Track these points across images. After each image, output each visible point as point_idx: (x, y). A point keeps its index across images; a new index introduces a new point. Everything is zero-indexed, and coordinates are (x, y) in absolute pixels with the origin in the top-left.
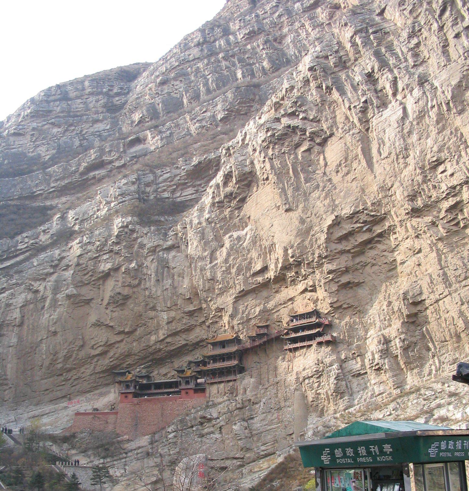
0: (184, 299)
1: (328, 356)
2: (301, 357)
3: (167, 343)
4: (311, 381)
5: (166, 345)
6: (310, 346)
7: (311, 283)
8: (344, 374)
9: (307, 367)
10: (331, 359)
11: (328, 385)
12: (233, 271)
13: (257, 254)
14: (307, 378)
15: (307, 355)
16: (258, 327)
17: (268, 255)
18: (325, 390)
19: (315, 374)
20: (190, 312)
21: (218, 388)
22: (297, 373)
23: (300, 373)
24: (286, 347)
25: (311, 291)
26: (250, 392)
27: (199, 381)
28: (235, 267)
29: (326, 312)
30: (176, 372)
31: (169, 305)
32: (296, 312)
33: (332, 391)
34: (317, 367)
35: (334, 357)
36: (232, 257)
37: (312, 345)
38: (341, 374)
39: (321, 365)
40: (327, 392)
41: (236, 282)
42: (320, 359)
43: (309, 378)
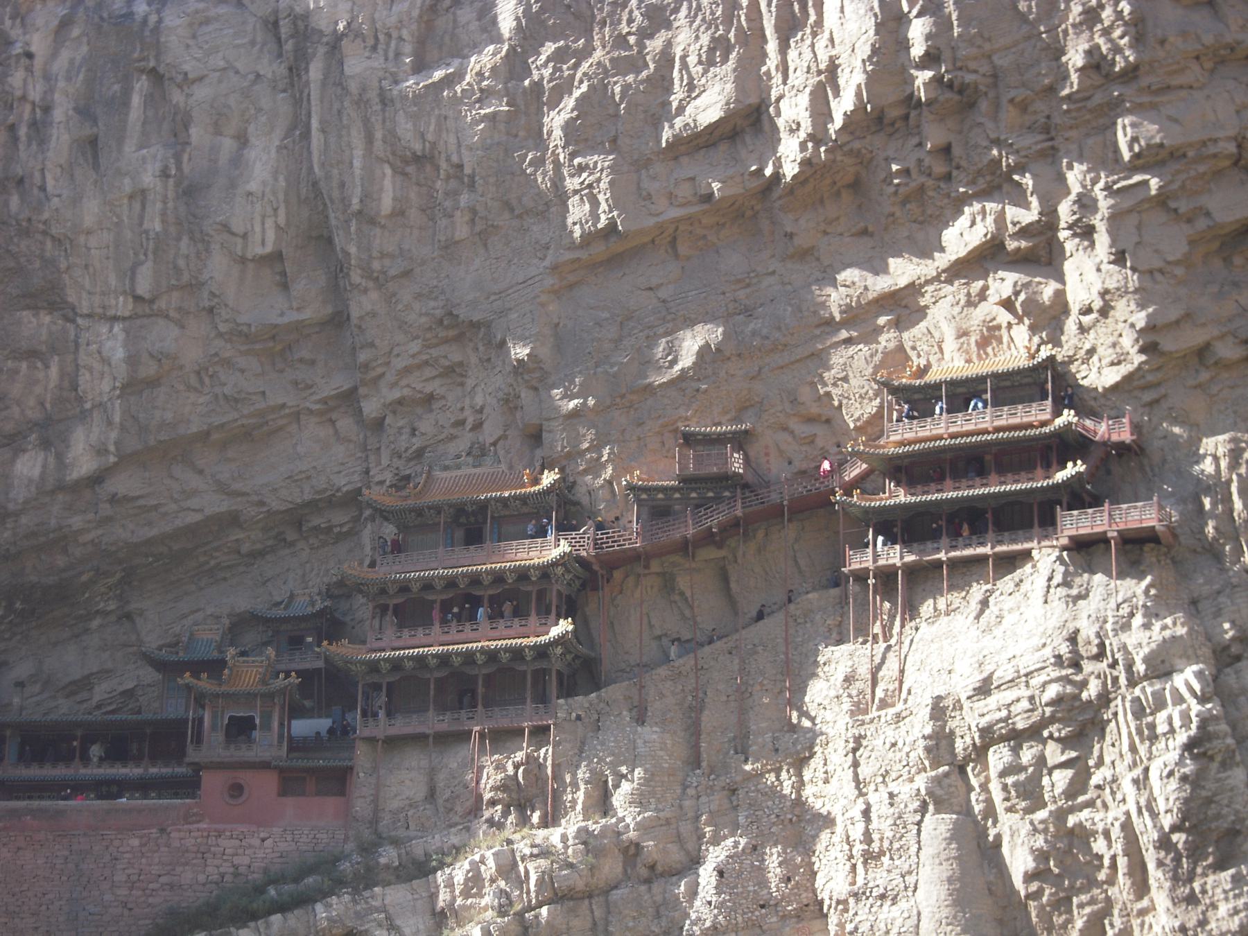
0: (243, 260)
1: (1138, 620)
2: (962, 622)
3: (114, 499)
4: (1027, 755)
5: (106, 509)
6: (1009, 563)
7: (1029, 216)
8: (1233, 726)
9: (1004, 673)
10: (1157, 633)
11: (1141, 783)
12: (556, 121)
13: (705, 39)
14: (1003, 739)
15: (993, 609)
16: (689, 439)
17: (772, 47)
18: (1116, 813)
19: (1052, 720)
20: (274, 332)
21: (432, 773)
22: (939, 711)
23: (958, 705)
24: (859, 561)
25: (1020, 261)
26: (639, 800)
27: (302, 727)
28: (569, 102)
29: (1111, 377)
30: (150, 675)
31: (144, 286)
32: (923, 371)
33: (1167, 821)
34: (1066, 680)
35: (1174, 626)
36: (549, 48)
37: (1026, 555)
38: (1223, 727)
39: (1088, 667)
40: (1127, 826)
41: (572, 183)
42: (1088, 631)
43: (1016, 738)
